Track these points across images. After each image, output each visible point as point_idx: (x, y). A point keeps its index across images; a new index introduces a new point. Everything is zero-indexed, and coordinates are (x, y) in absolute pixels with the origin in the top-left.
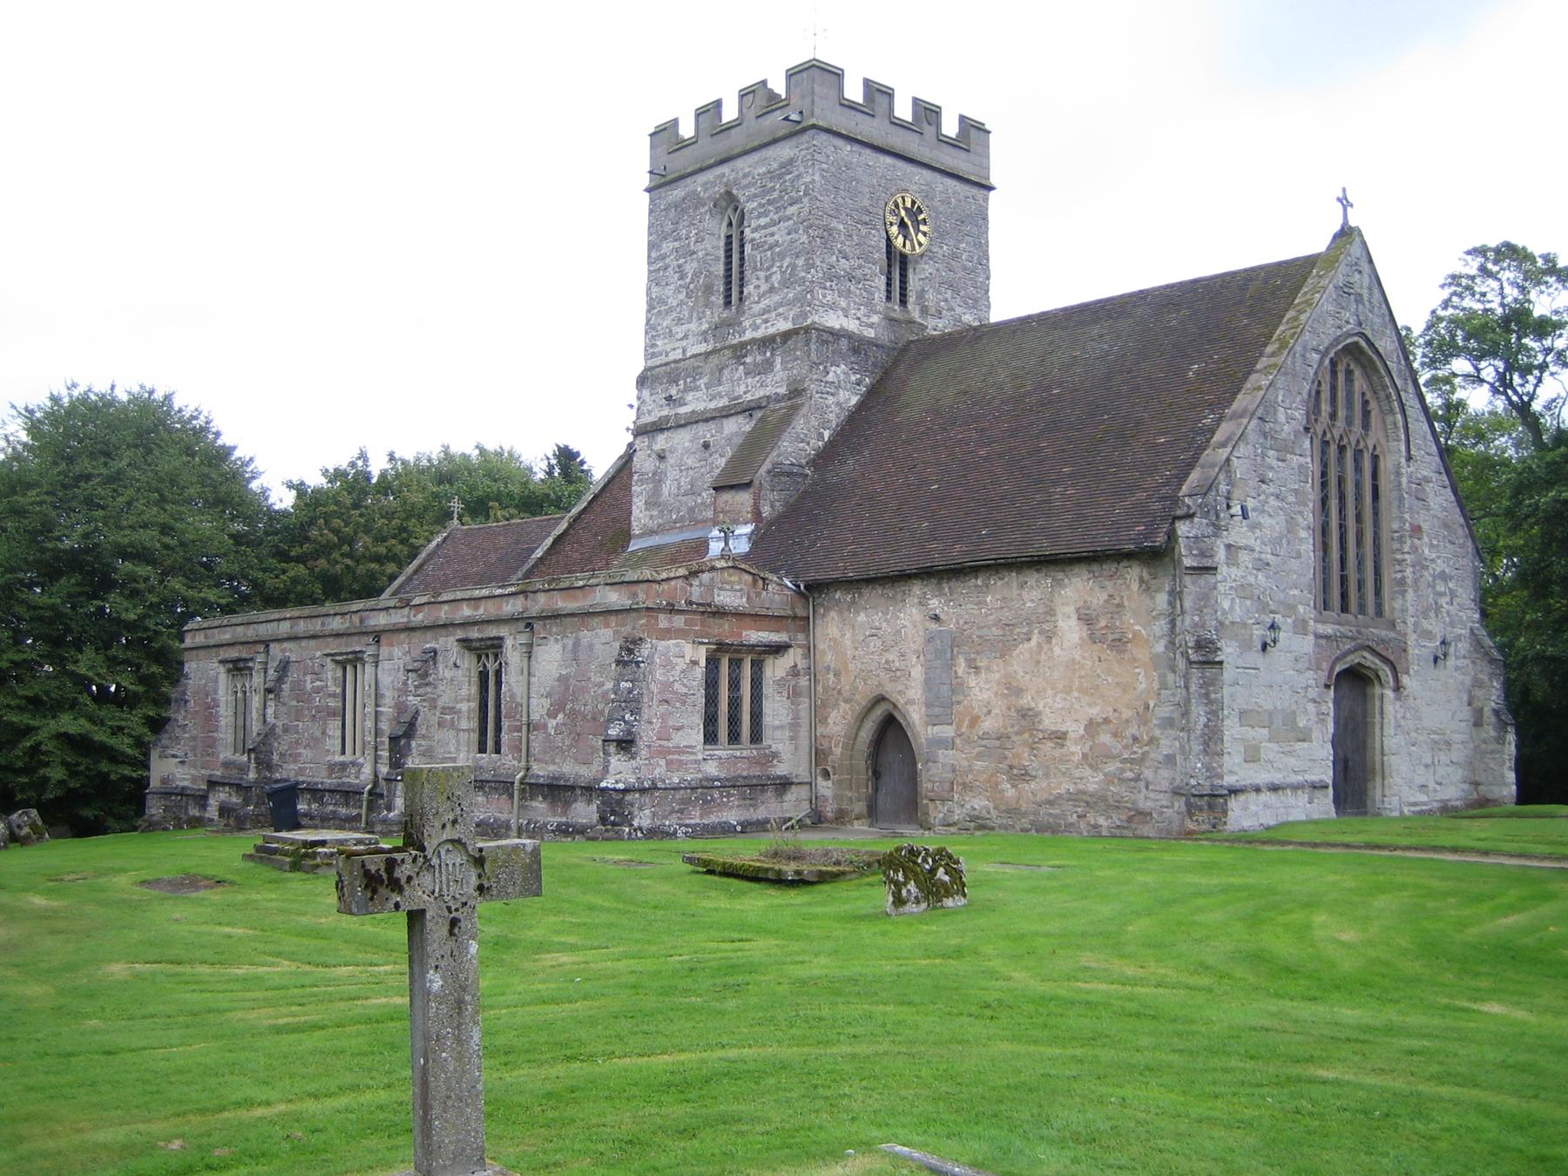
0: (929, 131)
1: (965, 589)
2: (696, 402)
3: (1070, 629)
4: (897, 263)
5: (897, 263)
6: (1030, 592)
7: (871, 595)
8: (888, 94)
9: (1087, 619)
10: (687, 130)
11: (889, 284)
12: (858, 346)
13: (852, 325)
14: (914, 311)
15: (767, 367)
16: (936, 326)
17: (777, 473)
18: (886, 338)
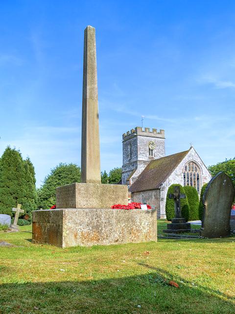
0: (155, 133)
1: (145, 192)
2: (127, 170)
3: (153, 197)
4: (151, 150)
5: (151, 150)
6: (150, 193)
7: (138, 193)
8: (149, 129)
9: (155, 196)
10: (126, 134)
11: (150, 153)
12: (144, 162)
13: (144, 159)
14: (153, 156)
15: (133, 166)
16: (156, 158)
17: (133, 178)
18: (149, 160)
